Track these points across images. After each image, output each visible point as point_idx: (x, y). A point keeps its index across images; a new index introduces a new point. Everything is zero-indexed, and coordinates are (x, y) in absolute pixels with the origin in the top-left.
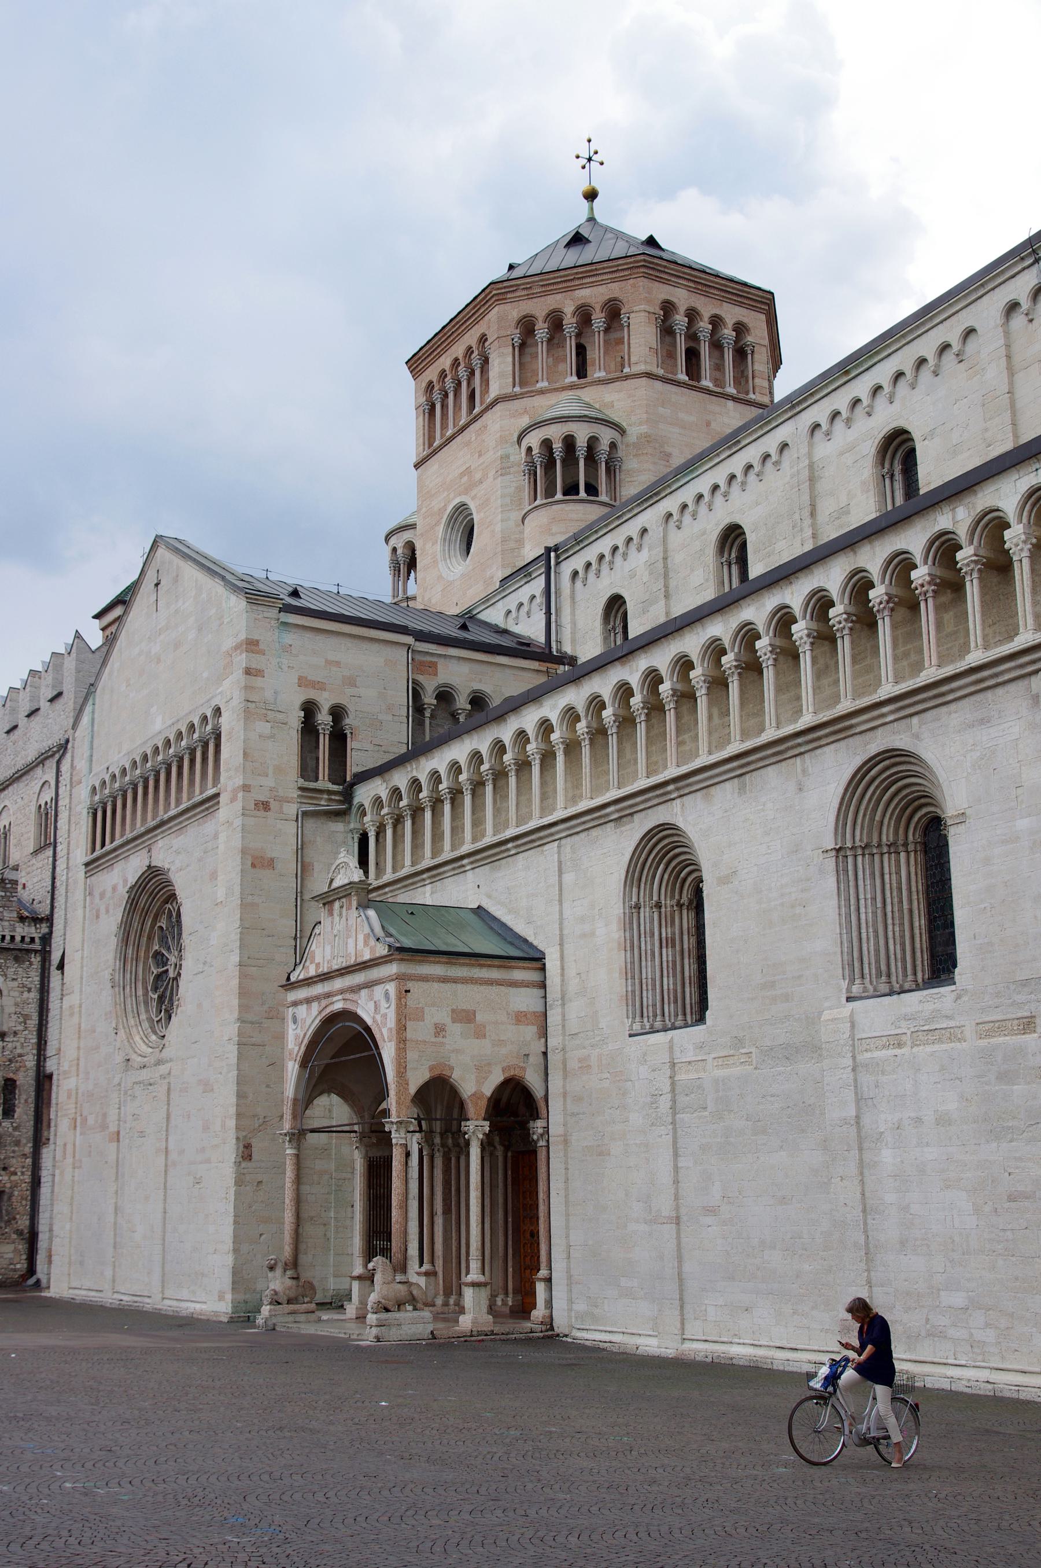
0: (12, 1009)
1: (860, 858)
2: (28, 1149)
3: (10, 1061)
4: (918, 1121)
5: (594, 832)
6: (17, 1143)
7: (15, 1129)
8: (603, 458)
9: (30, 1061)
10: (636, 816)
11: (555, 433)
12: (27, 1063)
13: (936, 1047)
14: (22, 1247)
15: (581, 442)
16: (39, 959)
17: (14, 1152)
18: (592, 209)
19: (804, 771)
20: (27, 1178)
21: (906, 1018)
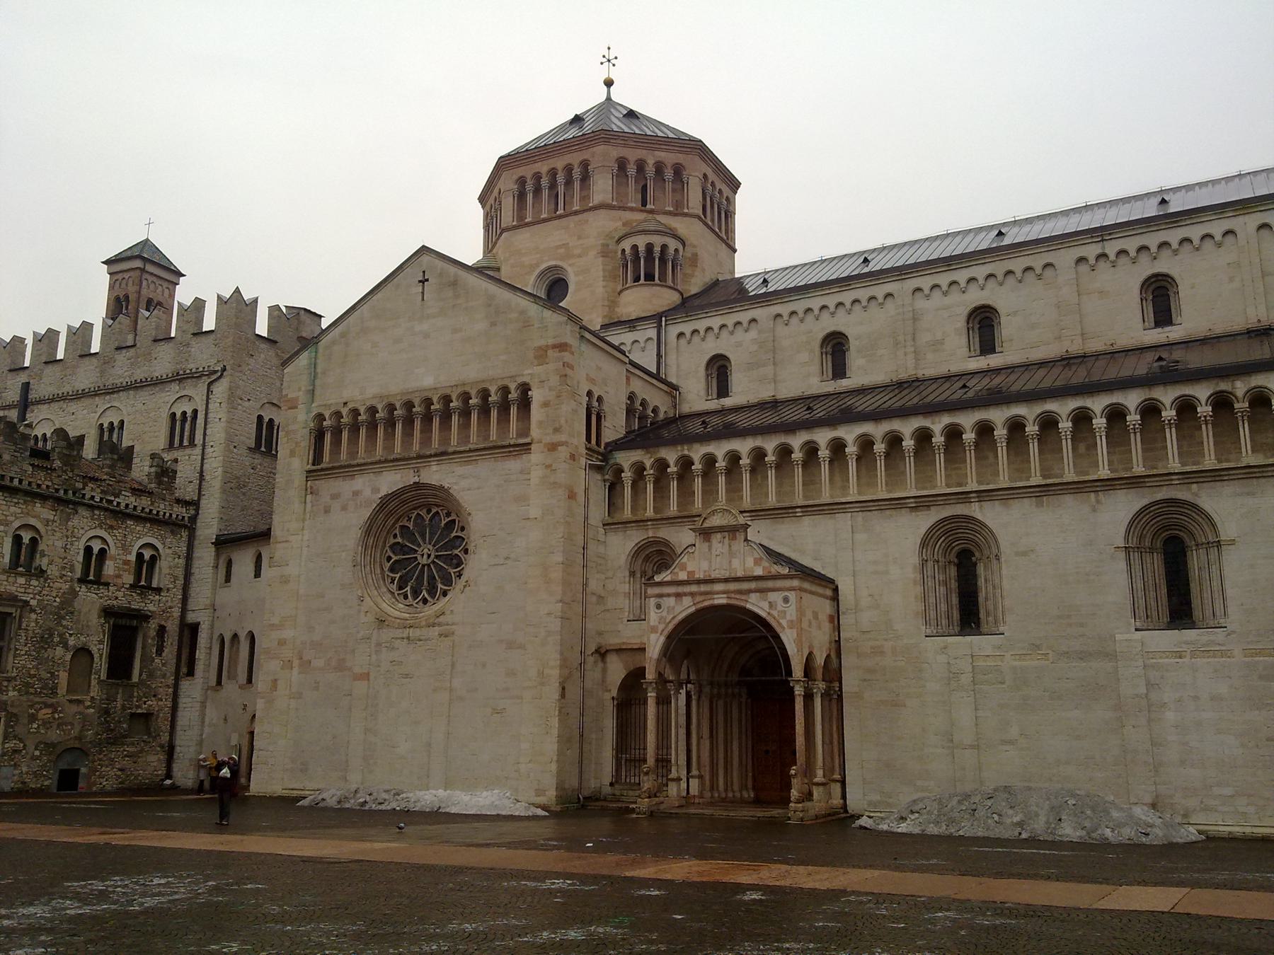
0: (167, 571)
1: (1131, 554)
2: (171, 681)
3: (163, 611)
4: (1196, 698)
5: (888, 512)
6: (164, 676)
7: (163, 665)
9: (176, 612)
10: (932, 508)
12: (174, 614)
13: (1210, 660)
14: (162, 757)
16: (187, 533)
17: (161, 682)
18: (609, 93)
19: (1098, 502)
20: (170, 705)
21: (1187, 643)
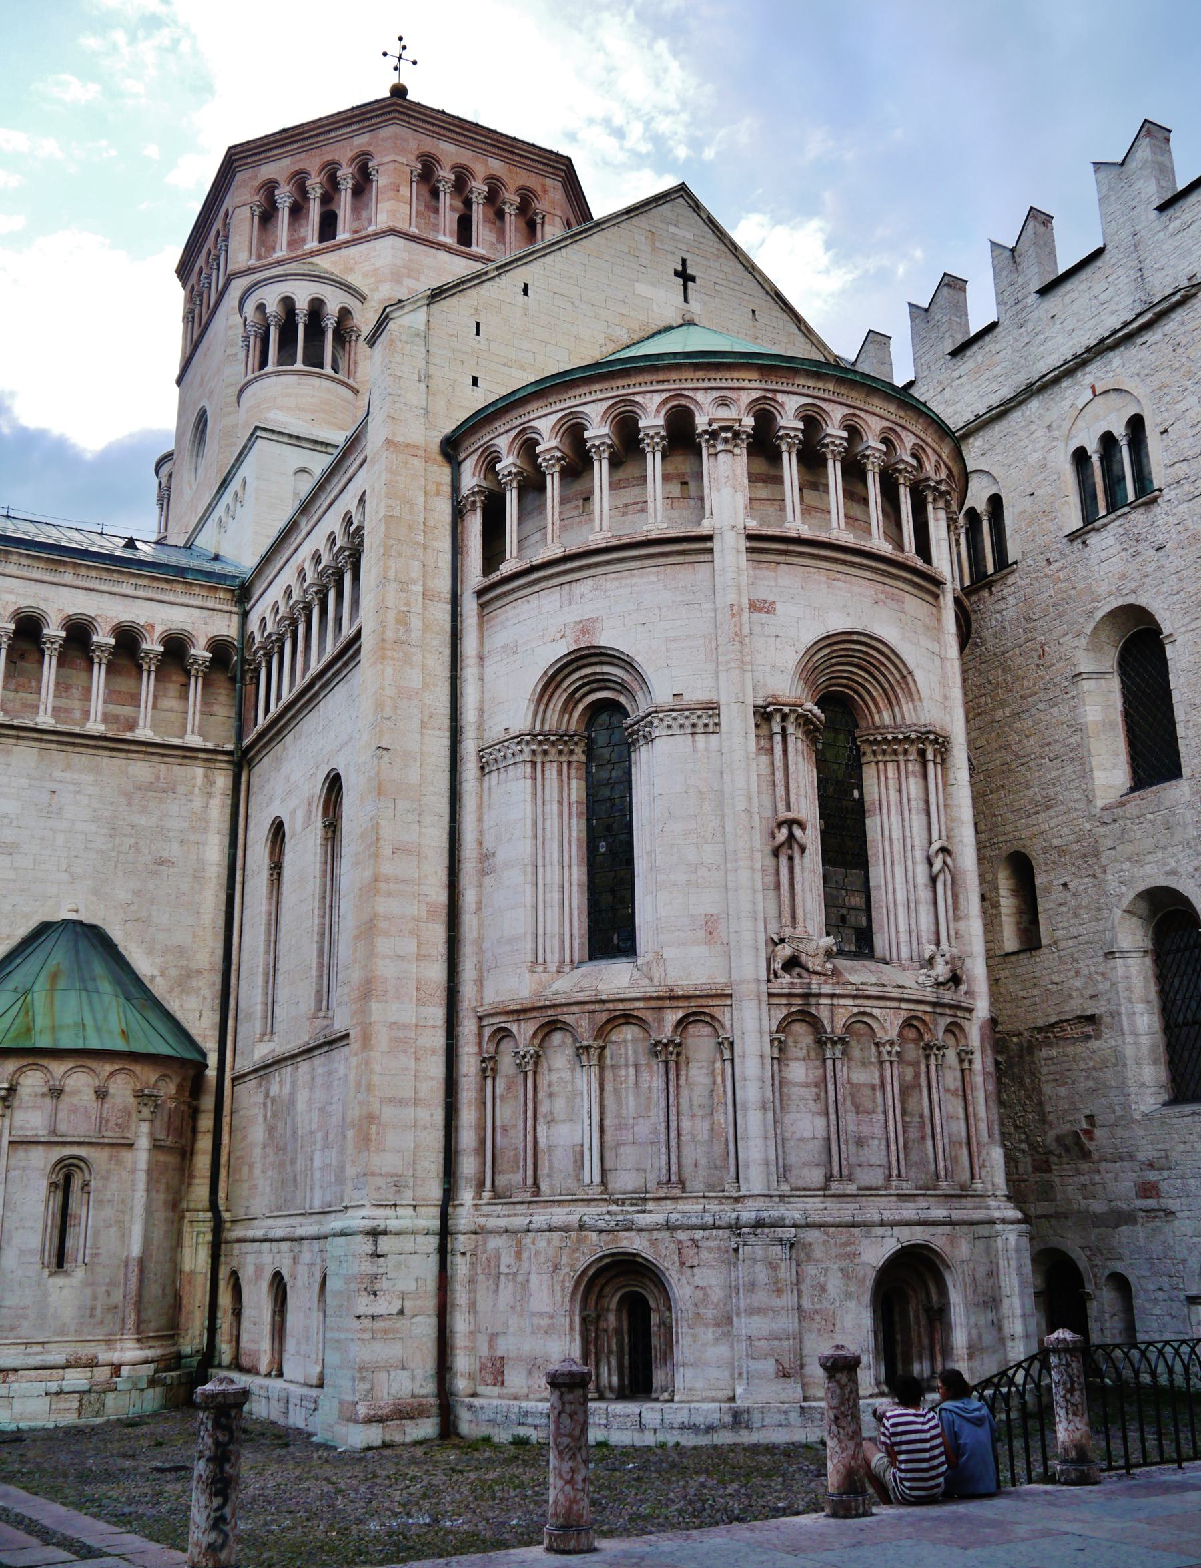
8: (330, 324)
11: (271, 297)
15: (302, 305)
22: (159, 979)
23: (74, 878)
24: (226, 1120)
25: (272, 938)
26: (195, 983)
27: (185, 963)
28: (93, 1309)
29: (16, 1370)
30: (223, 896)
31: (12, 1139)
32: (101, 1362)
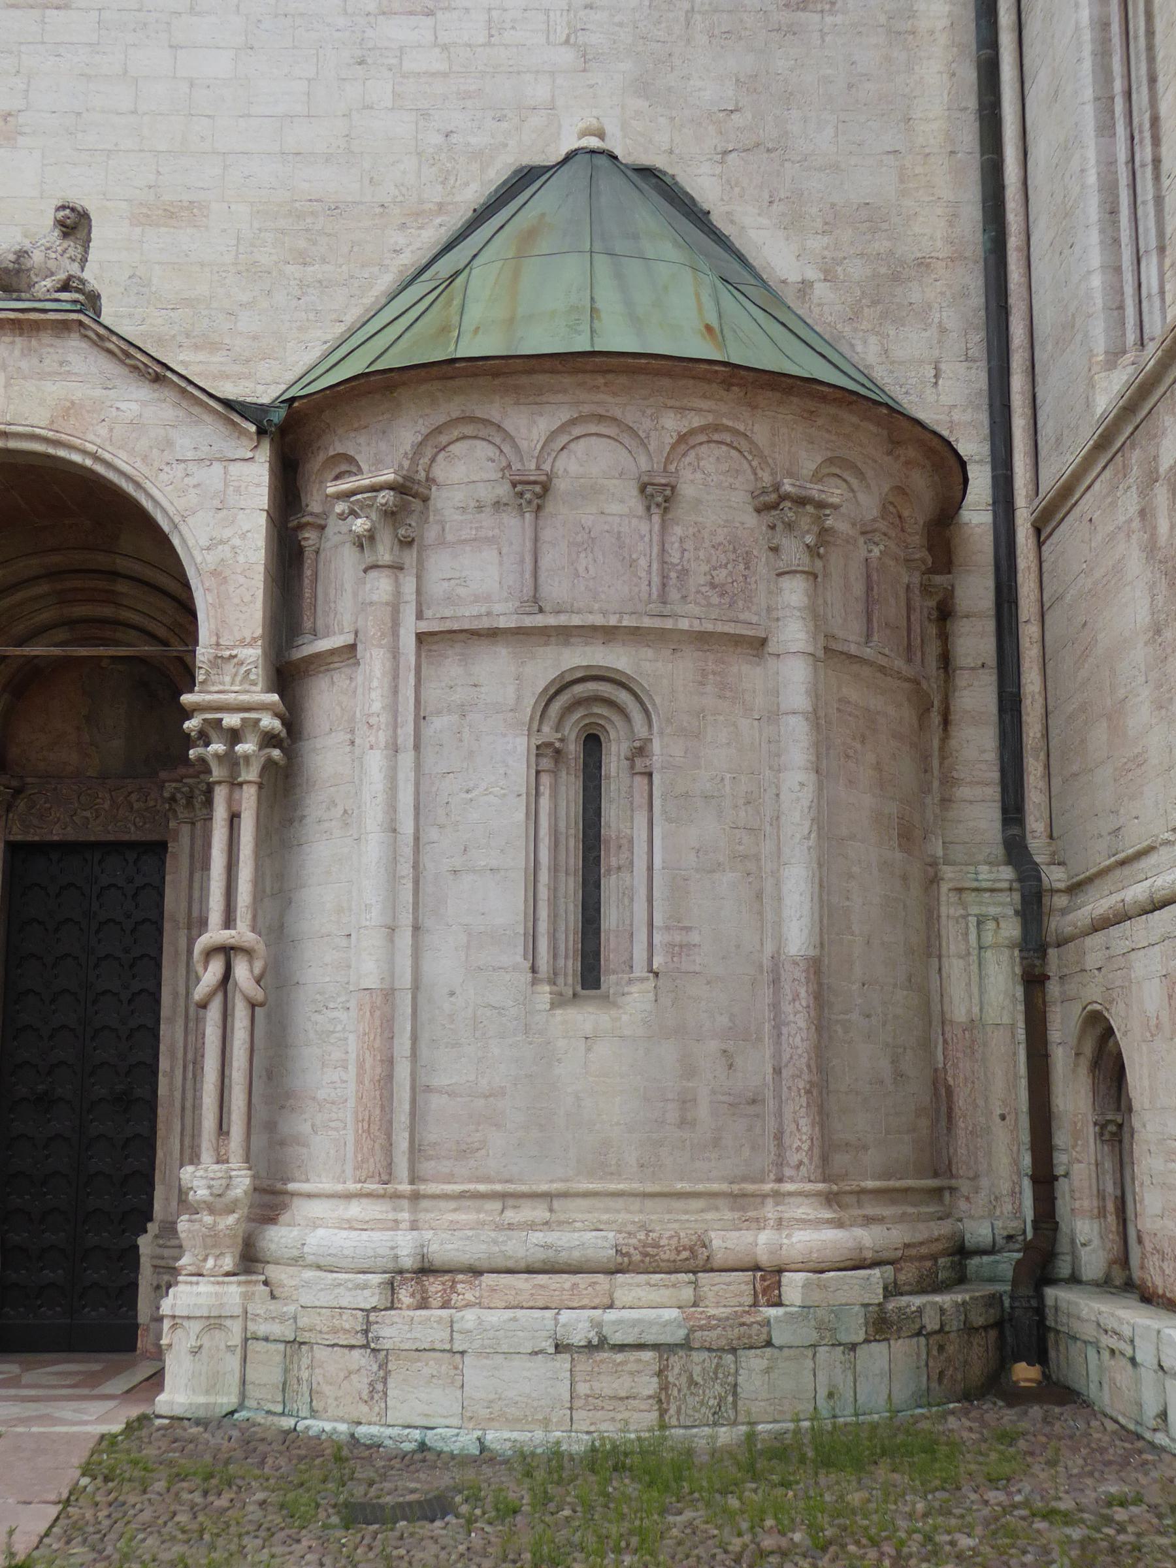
22: (821, 290)
23: (587, 59)
24: (1029, 632)
25: (1118, 86)
26: (916, 294)
27: (881, 245)
28: (686, 1101)
29: (476, 1272)
30: (969, 75)
31: (424, 627)
32: (719, 1259)
